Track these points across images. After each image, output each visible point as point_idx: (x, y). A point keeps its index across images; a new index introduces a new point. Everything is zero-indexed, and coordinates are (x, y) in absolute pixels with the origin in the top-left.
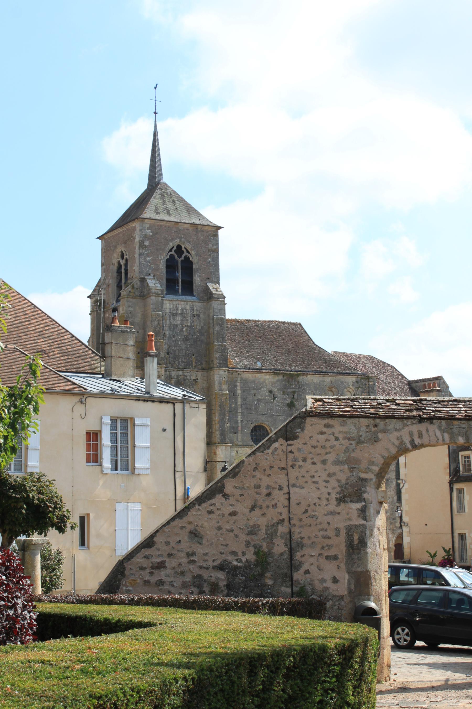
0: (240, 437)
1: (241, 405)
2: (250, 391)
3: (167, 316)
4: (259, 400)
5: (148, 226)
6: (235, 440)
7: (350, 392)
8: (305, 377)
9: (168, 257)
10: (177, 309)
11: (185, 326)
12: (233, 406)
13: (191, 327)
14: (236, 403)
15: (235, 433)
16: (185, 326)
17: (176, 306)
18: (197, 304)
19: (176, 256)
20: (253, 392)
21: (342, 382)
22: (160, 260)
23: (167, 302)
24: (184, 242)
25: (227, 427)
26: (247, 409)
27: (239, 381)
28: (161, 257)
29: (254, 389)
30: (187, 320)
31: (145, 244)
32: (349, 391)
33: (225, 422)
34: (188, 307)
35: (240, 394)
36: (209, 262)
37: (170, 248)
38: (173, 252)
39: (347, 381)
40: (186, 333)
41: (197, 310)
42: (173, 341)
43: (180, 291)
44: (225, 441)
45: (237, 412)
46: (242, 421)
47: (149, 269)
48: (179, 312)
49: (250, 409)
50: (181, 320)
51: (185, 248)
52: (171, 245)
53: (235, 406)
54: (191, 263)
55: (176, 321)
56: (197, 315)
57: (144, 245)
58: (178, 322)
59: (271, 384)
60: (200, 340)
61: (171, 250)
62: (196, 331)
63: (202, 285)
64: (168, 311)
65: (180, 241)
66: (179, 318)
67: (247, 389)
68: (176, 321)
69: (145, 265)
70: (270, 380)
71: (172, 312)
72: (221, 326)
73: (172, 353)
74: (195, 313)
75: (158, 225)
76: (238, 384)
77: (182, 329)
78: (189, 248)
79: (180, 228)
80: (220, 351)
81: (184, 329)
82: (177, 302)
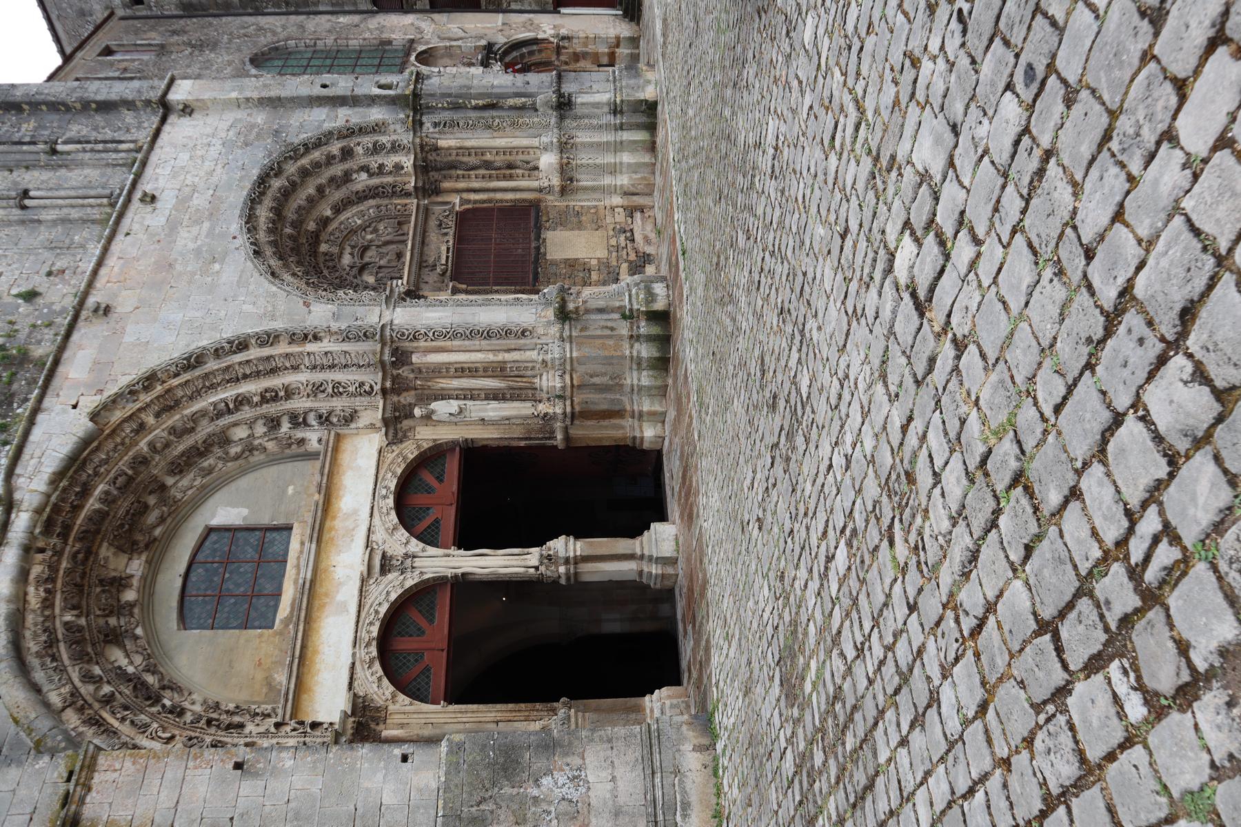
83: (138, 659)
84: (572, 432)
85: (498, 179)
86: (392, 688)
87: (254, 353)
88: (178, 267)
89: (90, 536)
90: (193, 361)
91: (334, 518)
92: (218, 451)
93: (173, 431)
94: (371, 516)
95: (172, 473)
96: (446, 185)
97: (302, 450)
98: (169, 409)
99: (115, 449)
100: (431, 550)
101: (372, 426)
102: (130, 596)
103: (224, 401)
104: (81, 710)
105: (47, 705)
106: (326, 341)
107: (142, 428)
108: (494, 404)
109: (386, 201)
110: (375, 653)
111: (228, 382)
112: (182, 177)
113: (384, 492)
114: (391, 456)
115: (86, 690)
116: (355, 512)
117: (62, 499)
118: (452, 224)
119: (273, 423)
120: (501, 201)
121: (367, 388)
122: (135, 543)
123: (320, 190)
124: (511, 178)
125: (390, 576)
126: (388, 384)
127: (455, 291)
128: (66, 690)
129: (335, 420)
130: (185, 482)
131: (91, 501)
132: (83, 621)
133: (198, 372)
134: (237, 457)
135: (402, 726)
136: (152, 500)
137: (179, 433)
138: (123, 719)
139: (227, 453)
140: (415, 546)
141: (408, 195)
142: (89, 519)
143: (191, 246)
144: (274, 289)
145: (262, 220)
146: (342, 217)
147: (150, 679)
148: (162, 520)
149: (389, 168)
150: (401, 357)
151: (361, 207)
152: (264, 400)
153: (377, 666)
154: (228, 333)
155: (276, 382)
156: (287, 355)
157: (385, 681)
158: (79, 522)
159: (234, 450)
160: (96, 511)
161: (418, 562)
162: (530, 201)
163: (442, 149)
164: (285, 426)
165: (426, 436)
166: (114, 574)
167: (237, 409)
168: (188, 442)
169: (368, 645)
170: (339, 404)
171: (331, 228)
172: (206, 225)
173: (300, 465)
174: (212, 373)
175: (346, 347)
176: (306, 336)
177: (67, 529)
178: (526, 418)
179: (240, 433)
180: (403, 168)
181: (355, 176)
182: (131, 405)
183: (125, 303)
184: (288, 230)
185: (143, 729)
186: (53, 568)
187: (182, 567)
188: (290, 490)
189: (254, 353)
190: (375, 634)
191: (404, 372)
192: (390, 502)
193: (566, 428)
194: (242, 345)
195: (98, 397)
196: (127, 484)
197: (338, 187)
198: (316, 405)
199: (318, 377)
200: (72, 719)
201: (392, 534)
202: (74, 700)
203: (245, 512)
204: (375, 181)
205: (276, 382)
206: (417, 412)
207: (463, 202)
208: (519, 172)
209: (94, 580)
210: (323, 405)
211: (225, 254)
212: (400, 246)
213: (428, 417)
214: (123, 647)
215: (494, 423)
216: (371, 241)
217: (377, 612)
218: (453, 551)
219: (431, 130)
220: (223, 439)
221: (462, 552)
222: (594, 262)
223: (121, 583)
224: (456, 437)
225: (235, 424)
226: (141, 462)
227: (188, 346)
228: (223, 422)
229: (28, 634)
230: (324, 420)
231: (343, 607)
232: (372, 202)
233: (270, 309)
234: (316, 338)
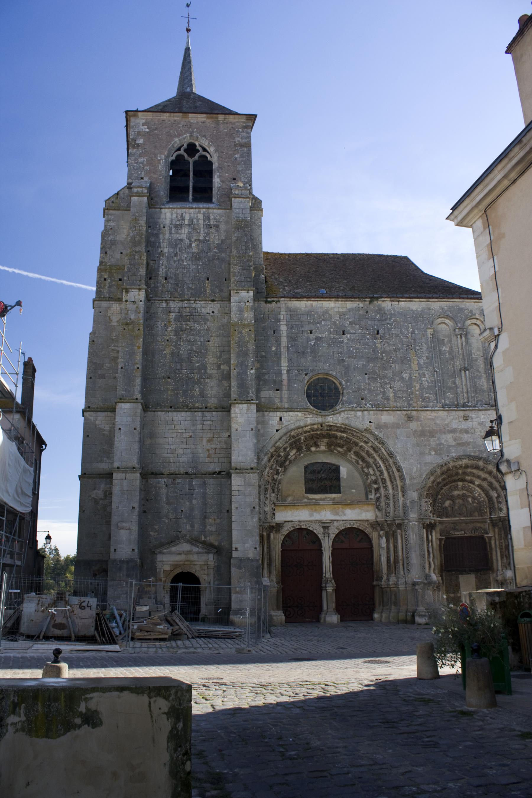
0: (286, 396)
1: (288, 348)
2: (302, 326)
3: (167, 229)
4: (317, 339)
5: (144, 121)
6: (277, 401)
7: (478, 326)
8: (397, 303)
9: (174, 158)
10: (183, 219)
11: (195, 240)
12: (274, 349)
13: (204, 241)
14: (279, 345)
15: (278, 390)
16: (195, 240)
17: (182, 216)
18: (215, 211)
19: (186, 155)
20: (307, 328)
21: (461, 310)
22: (160, 160)
23: (166, 210)
24: (197, 137)
25: (251, 374)
26: (297, 352)
27: (283, 313)
28: (160, 157)
29: (309, 323)
30: (199, 233)
31: (137, 142)
32: (476, 324)
33: (247, 366)
34: (201, 216)
35: (285, 332)
36: (236, 158)
37: (176, 146)
38: (182, 152)
39: (470, 308)
40: (196, 250)
41: (214, 219)
42: (175, 262)
43: (191, 197)
44: (247, 397)
45: (280, 357)
46: (288, 371)
47: (142, 172)
48: (187, 222)
49: (303, 353)
50: (189, 233)
51: (200, 146)
52: (177, 142)
53: (277, 349)
54: (211, 163)
55: (181, 234)
56: (214, 226)
57: (135, 144)
58: (184, 236)
59: (338, 316)
60: (218, 259)
61: (179, 149)
62: (212, 246)
63: (224, 187)
64: (168, 222)
65: (191, 136)
66: (185, 231)
67: (297, 323)
68: (181, 234)
69: (136, 168)
70: (336, 310)
71: (174, 222)
72: (244, 231)
73: (172, 278)
74: (212, 223)
75: (159, 120)
76: (282, 317)
77: (190, 244)
78: (206, 144)
79: (192, 121)
80: (241, 264)
81: (194, 245)
82: (184, 210)
83: (293, 457)
84: (377, 587)
85: (501, 552)
86: (286, 534)
87: (397, 474)
88: (432, 439)
89: (329, 436)
90: (391, 455)
91: (343, 508)
92: (364, 465)
93: (368, 451)
94: (343, 521)
95: (355, 452)
96: (497, 530)
97: (368, 493)
98: (374, 449)
99: (358, 437)
100: (331, 542)
101: (377, 516)
102: (313, 449)
103: (380, 466)
104: (275, 451)
105: (276, 443)
106: (403, 499)
107: (366, 443)
108: (385, 559)
109: (487, 505)
110: (296, 528)
111: (387, 467)
112: (479, 427)
113: (352, 524)
114: (366, 524)
115: (282, 450)
116: (345, 515)
117: (338, 427)
118: (477, 534)
119: (375, 482)
120: (491, 554)
121: (388, 515)
122: (330, 446)
123: (485, 479)
124: (502, 557)
125: (322, 530)
126: (389, 522)
127: (440, 540)
128: (281, 445)
129: (378, 504)
130: (353, 456)
131: (340, 434)
132: (302, 441)
133: (388, 457)
134: (364, 471)
135: (274, 538)
136: (345, 448)
137: (368, 453)
138: (273, 462)
139: (364, 468)
140: (332, 536)
141: (491, 514)
142: (334, 434)
143: (443, 441)
144: (424, 476)
146: (477, 488)
147: (287, 463)
148: (339, 452)
150: (399, 526)
151: (483, 495)
152: (382, 479)
153: (292, 529)
155: (388, 483)
156: (397, 486)
157: (288, 532)
158: (333, 432)
159: (366, 470)
160: (337, 436)
161: (327, 538)
162: (492, 566)
164: (375, 486)
165: (374, 535)
166: (319, 444)
167: (378, 470)
168: (366, 456)
169: (299, 525)
170: (383, 504)
171: (471, 485)
173: (363, 491)
174: (388, 462)
175: (401, 506)
176: (403, 492)
177: (330, 430)
178: (382, 571)
179: (371, 472)
180: (501, 511)
182: (373, 438)
183: (414, 425)
185: (271, 468)
186: (317, 430)
187: (325, 461)
188: (354, 491)
189: (397, 474)
190: (302, 527)
191: (394, 528)
192: (349, 526)
193: (379, 585)
194: (399, 470)
195: (374, 429)
196: (348, 441)
197: (488, 485)
198: (383, 497)
199: (391, 497)
200: (272, 451)
201: (336, 528)
202: (277, 449)
203: (345, 477)
204: (495, 500)
205: (388, 483)
206: (381, 533)
207: (490, 538)
208: (505, 561)
209: (315, 440)
210: (383, 499)
211: (440, 454)
212: (465, 514)
213: (380, 536)
214: (297, 452)
215: (380, 559)
216: (468, 502)
217: (310, 527)
218: (331, 549)
220: (368, 466)
221: (330, 552)
222: (459, 595)
223: (317, 446)
224: (374, 546)
225: (374, 470)
226: (356, 444)
227: (397, 452)
228: (374, 465)
229: (296, 431)
230: (378, 499)
231: (311, 515)
232: (486, 499)
234: (403, 496)
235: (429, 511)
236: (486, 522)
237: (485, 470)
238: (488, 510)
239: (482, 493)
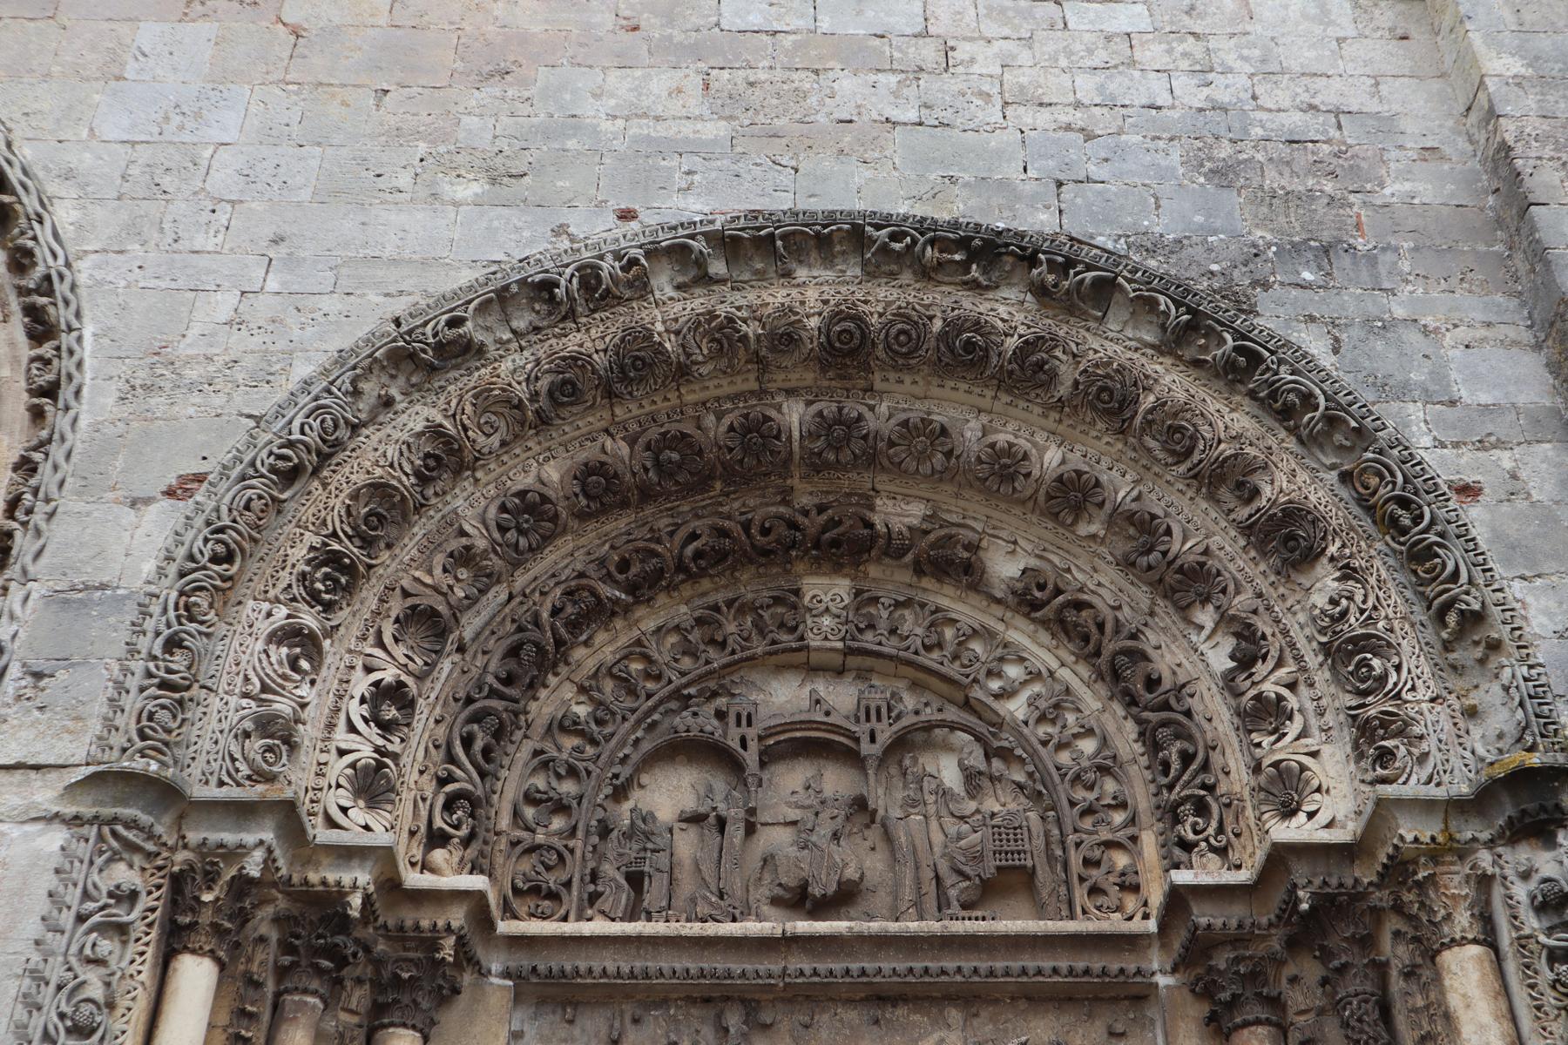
88: (475, 99)
109: (1142, 798)
112: (991, 28)
143: (590, 110)
144: (303, 369)
145: (776, 296)
146: (1020, 634)
149: (1283, 749)
151: (1092, 700)
154: (84, 271)
163: (1437, 979)
171: (945, 598)
172: (715, 130)
181: (1206, 617)
184: (794, 415)
197: (1127, 564)
219: (1521, 891)
227: (68, 175)
232: (1126, 740)
233: (192, 374)
235: (338, 768)
236: (1138, 995)
237: (1067, 373)
238: (1149, 843)
239: (1075, 676)
